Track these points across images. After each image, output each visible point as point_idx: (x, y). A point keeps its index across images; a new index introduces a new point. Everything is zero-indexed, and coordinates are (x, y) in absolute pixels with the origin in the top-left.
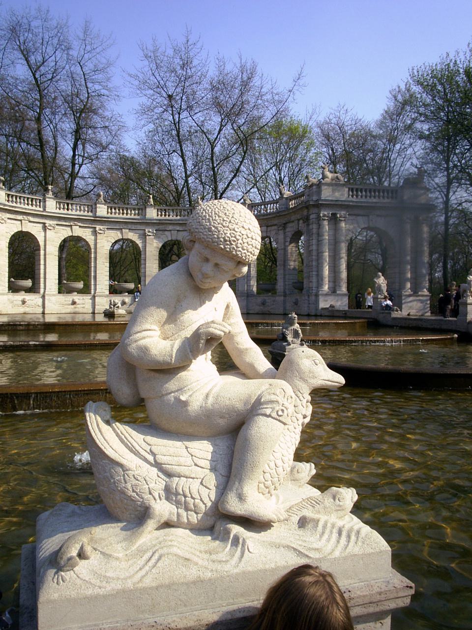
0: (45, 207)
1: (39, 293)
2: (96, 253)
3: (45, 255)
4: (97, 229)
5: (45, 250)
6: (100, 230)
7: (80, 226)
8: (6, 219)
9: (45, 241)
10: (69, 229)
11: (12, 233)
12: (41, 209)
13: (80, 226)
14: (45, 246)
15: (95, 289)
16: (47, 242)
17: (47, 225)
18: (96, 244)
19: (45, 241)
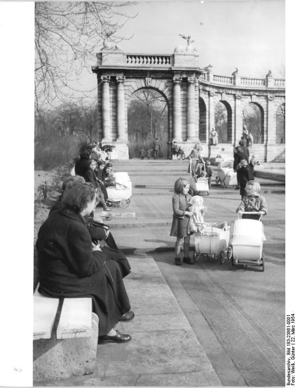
0: (234, 84)
1: (231, 143)
2: (267, 114)
3: (235, 117)
4: (269, 97)
5: (235, 113)
6: (271, 97)
7: (257, 96)
8: (214, 93)
9: (235, 107)
10: (249, 97)
11: (230, 103)
12: (232, 84)
13: (257, 96)
14: (235, 110)
15: (267, 140)
16: (237, 108)
17: (236, 96)
18: (267, 108)
19: (235, 107)
